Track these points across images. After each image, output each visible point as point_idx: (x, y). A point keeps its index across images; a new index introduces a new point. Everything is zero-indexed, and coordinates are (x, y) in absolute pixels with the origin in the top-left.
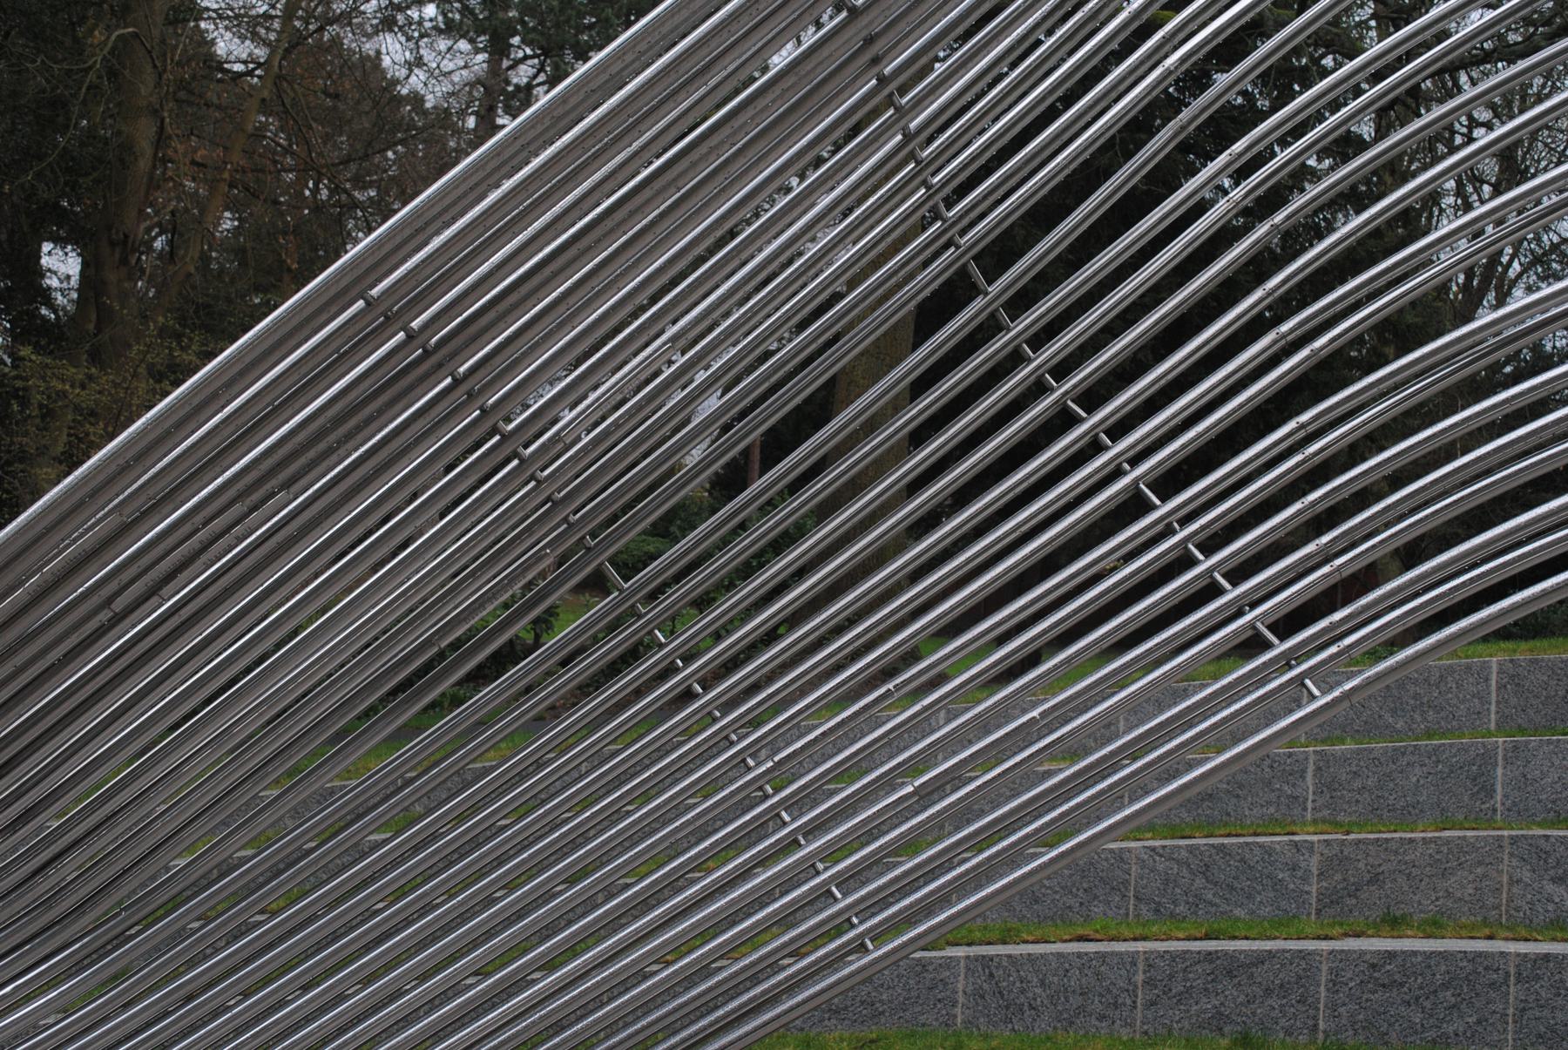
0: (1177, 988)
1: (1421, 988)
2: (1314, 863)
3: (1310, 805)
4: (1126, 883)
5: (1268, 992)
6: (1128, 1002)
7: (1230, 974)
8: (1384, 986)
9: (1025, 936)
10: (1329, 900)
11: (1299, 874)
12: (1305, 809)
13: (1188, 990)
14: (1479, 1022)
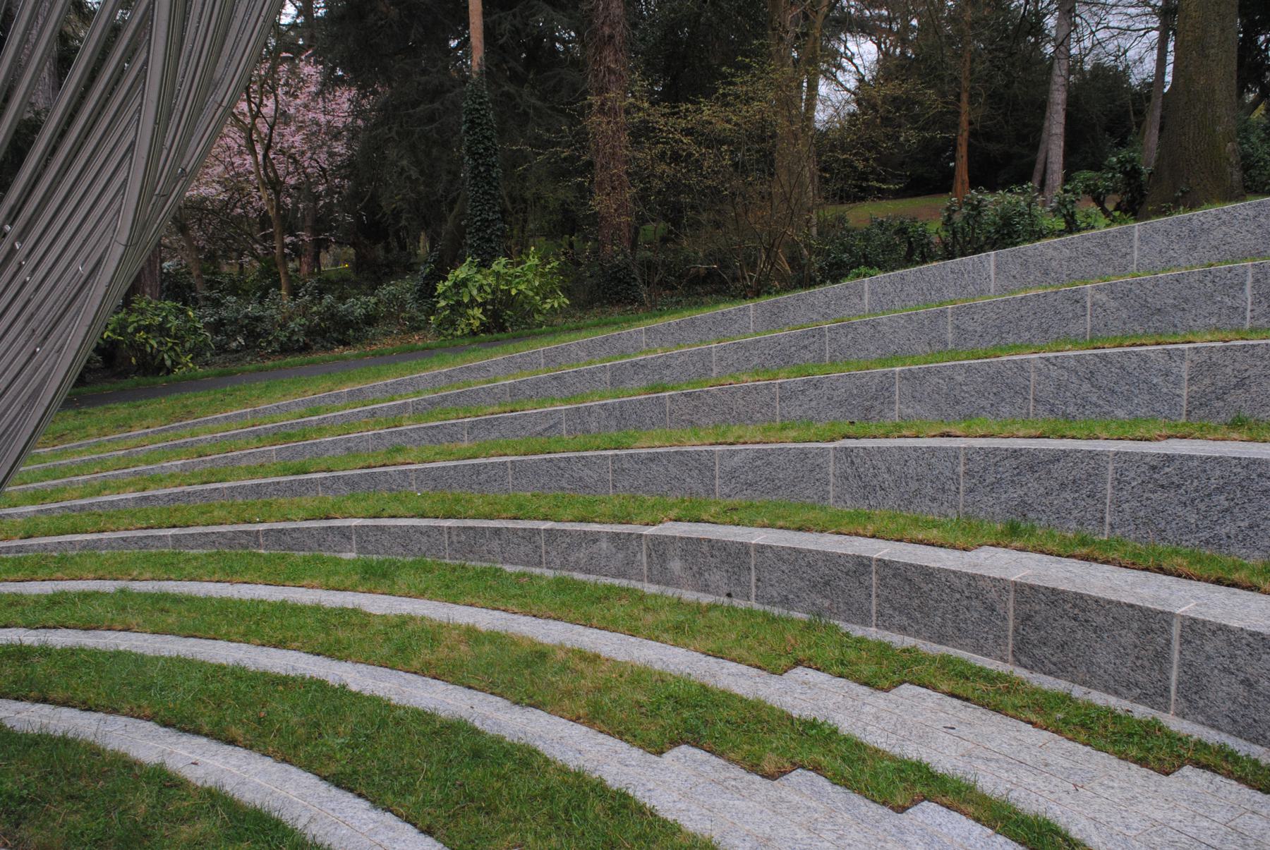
0: (990, 479)
1: (1196, 491)
2: (1185, 370)
3: (1248, 314)
4: (1026, 388)
5: (1063, 486)
6: (953, 488)
7: (1032, 469)
8: (1162, 486)
9: (904, 433)
10: (1199, 403)
11: (1172, 379)
12: (1244, 318)
13: (999, 481)
14: (1251, 527)
